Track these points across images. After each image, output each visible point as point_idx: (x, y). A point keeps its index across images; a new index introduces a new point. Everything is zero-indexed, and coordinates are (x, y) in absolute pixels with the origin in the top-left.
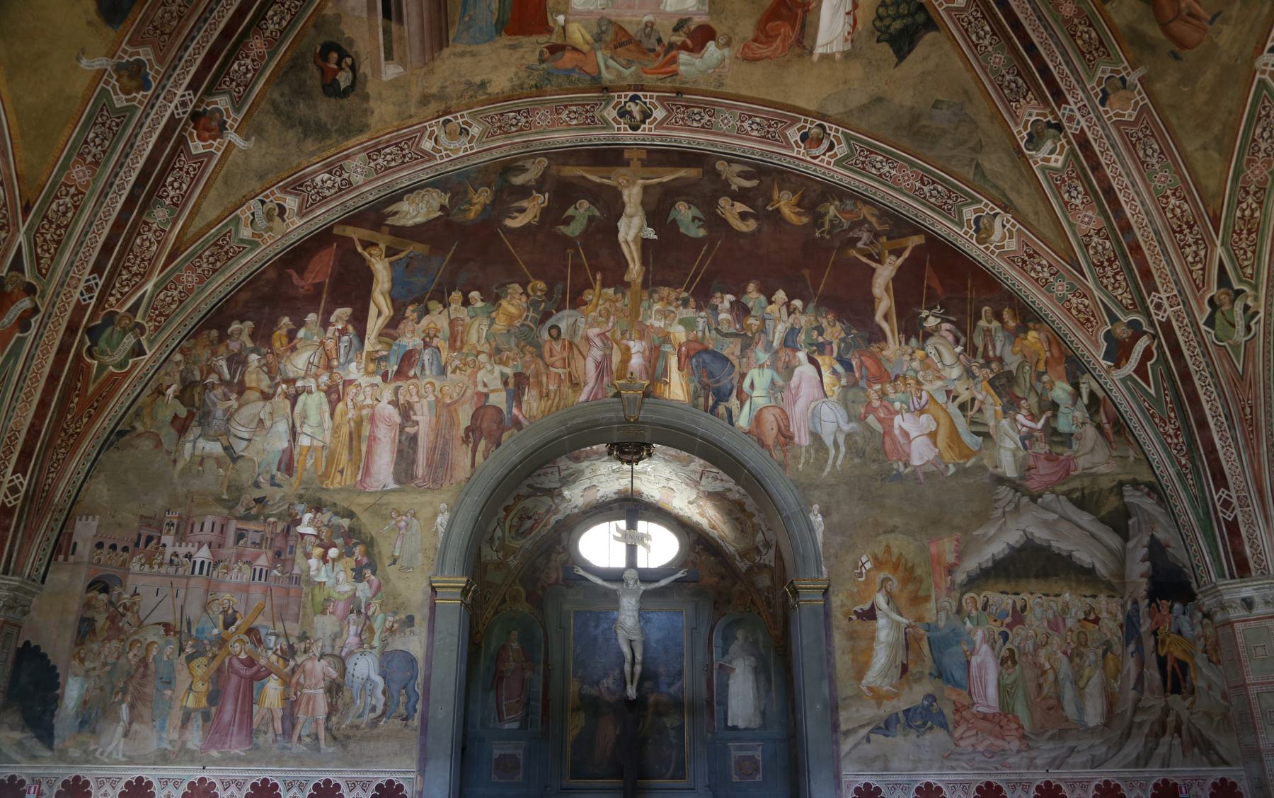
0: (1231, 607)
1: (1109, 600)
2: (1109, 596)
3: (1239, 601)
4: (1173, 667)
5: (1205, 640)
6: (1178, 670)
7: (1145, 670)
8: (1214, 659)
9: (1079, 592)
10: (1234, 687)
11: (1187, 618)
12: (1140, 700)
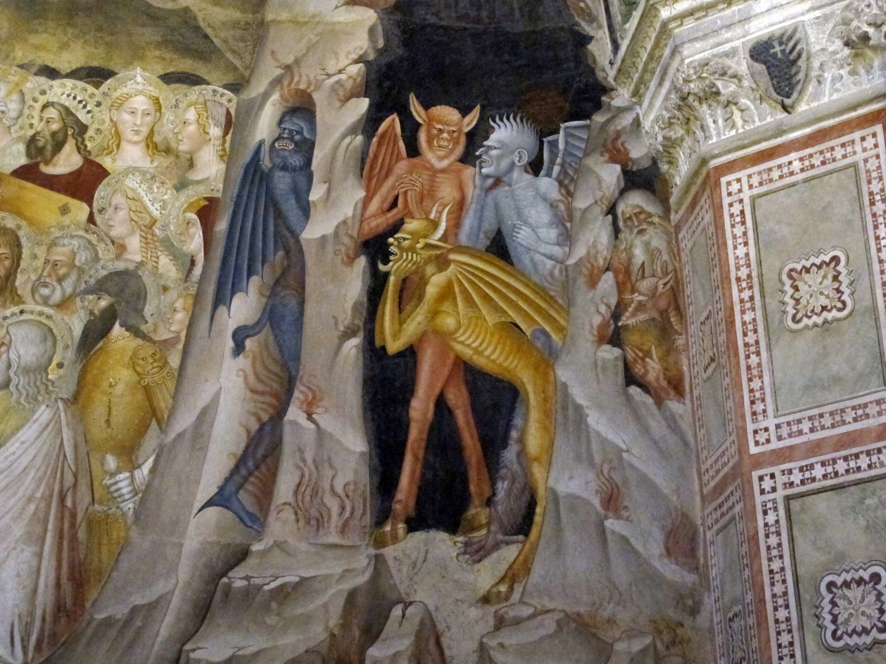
0: (712, 95)
1: (168, 94)
2: (168, 78)
4: (441, 404)
5: (621, 287)
6: (463, 418)
7: (295, 413)
8: (653, 369)
9: (20, 54)
11: (547, 184)
12: (241, 555)
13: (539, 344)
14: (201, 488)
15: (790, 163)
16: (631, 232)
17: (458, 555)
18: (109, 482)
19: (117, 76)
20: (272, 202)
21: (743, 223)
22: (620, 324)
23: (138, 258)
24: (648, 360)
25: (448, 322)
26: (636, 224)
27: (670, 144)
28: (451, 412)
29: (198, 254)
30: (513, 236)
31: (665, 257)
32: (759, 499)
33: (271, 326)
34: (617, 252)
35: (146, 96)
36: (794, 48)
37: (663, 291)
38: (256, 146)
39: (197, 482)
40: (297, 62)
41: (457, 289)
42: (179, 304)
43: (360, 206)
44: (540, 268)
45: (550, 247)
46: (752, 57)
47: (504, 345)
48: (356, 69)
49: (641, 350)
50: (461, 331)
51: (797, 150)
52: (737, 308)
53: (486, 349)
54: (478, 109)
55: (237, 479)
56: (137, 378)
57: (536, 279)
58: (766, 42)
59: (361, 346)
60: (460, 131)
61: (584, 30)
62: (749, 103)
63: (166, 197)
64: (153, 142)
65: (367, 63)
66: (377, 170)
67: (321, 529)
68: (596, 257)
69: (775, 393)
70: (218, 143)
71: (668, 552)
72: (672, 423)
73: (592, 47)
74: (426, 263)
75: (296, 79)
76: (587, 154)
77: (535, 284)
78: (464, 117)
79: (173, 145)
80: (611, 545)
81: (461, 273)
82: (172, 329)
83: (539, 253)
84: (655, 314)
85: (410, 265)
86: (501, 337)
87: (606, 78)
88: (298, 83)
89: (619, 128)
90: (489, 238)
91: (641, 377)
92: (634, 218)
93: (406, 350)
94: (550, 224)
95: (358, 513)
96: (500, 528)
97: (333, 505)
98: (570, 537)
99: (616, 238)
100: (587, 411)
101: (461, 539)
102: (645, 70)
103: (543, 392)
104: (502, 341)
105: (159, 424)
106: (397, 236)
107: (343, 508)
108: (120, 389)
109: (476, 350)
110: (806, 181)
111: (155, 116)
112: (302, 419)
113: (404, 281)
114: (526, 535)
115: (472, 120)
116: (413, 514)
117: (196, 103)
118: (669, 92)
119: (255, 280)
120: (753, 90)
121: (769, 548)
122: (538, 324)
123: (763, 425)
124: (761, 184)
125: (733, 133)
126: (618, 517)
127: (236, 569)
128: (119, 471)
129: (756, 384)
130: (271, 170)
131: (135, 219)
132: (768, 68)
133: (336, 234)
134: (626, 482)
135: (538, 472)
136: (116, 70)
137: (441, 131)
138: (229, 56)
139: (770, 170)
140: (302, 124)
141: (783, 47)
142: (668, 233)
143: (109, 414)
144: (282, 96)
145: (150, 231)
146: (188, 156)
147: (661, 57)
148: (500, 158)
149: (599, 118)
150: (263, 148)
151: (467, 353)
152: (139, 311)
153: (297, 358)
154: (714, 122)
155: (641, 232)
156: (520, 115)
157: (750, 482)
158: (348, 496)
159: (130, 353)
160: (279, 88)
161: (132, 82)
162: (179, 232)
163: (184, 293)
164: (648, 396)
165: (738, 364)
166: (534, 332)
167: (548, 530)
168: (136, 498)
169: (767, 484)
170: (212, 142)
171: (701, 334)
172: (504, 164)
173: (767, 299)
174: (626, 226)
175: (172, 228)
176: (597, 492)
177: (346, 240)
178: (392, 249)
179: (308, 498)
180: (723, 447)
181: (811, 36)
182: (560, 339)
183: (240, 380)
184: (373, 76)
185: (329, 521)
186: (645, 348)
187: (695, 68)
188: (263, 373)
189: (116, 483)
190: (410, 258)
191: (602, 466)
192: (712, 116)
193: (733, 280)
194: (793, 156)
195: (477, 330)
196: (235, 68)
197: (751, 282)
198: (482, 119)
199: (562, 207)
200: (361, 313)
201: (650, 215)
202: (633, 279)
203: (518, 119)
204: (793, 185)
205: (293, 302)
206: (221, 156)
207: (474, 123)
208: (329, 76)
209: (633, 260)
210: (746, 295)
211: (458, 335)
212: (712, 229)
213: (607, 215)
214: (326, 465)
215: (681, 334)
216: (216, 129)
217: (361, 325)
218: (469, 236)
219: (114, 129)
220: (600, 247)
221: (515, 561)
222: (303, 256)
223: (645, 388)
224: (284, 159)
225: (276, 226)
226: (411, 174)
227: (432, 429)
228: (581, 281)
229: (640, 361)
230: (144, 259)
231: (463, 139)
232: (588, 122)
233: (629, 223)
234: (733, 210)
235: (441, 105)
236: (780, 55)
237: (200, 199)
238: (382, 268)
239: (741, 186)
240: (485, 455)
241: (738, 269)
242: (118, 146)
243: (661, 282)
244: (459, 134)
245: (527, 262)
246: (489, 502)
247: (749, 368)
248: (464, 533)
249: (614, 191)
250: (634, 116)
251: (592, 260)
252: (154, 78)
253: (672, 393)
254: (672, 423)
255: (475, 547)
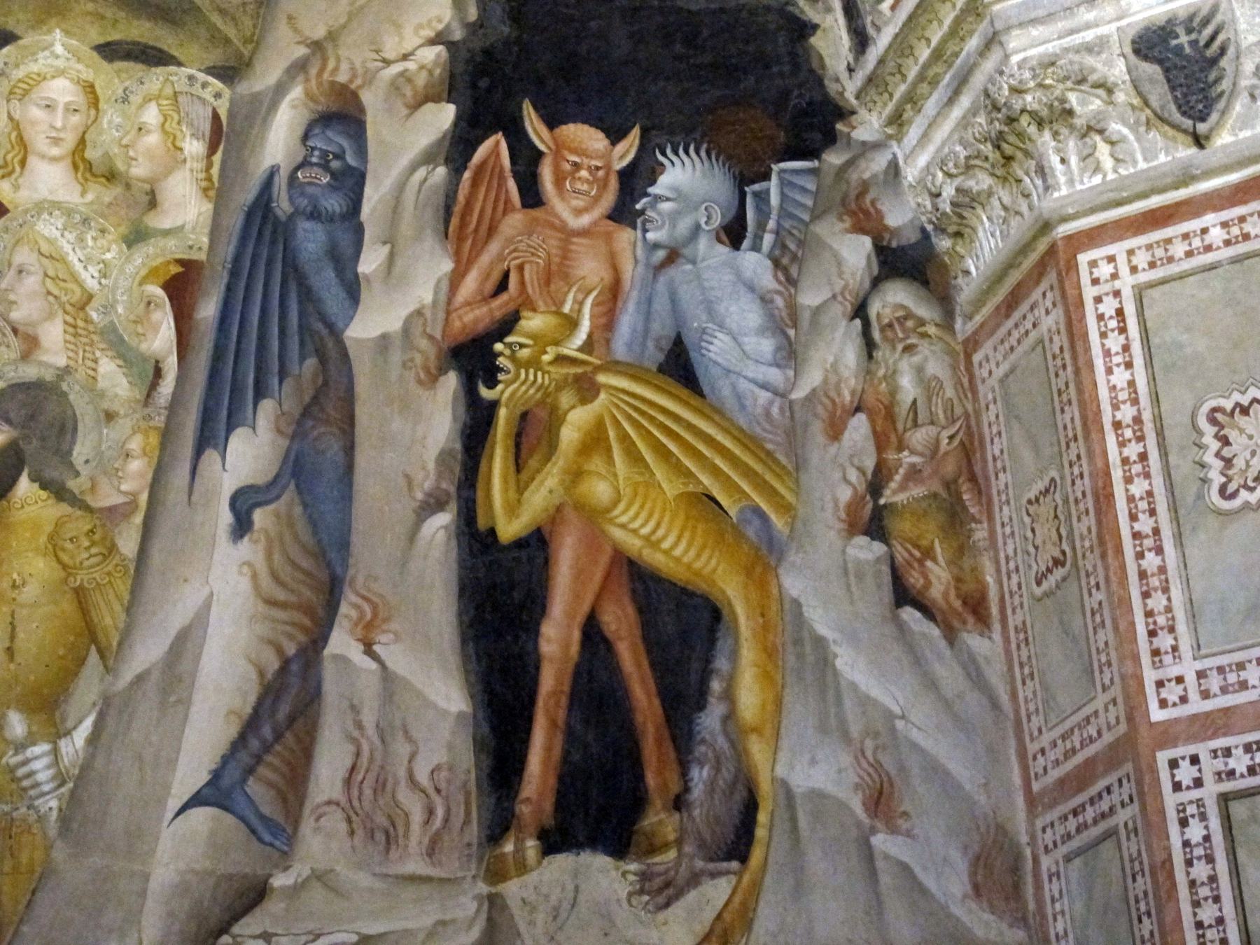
1: (110, 77)
2: (109, 51)
3: (1118, 71)
4: (593, 634)
5: (880, 441)
7: (342, 642)
10: (1067, 786)
13: (751, 532)
14: (179, 774)
15: (1205, 231)
16: (894, 348)
17: (630, 895)
18: (14, 761)
19: (21, 42)
20: (294, 271)
21: (1123, 330)
22: (882, 501)
23: (62, 361)
24: (929, 564)
25: (599, 490)
26: (901, 335)
27: (967, 201)
28: (608, 645)
29: (166, 357)
30: (701, 348)
31: (950, 392)
32: (1171, 800)
33: (297, 486)
34: (872, 379)
35: (72, 80)
36: (1213, 38)
37: (949, 448)
38: (265, 176)
39: (172, 763)
40: (332, 36)
41: (612, 434)
42: (135, 444)
43: (445, 286)
44: (748, 403)
45: (763, 368)
46: (1137, 52)
47: (695, 527)
48: (432, 54)
49: (917, 547)
50: (621, 506)
51: (1216, 209)
52: (1117, 474)
53: (664, 537)
54: (636, 133)
55: (244, 757)
56: (63, 574)
57: (742, 422)
58: (1162, 28)
59: (453, 528)
60: (608, 167)
61: (802, 12)
62: (1125, 131)
63: (108, 256)
64: (84, 159)
65: (451, 46)
66: (472, 226)
67: (393, 847)
68: (838, 384)
69: (1193, 616)
70: (200, 165)
71: (977, 889)
72: (974, 672)
73: (817, 41)
74: (559, 388)
75: (331, 64)
76: (817, 215)
77: (741, 430)
78: (614, 143)
79: (120, 166)
80: (885, 880)
81: (618, 407)
82: (124, 487)
83: (745, 377)
84: (937, 487)
85: (532, 391)
86: (687, 518)
87: (842, 94)
88: (336, 69)
89: (866, 175)
90: (661, 349)
91: (919, 592)
92: (897, 326)
93: (531, 535)
94: (761, 331)
95: (458, 820)
96: (699, 846)
97: (414, 807)
98: (816, 862)
99: (870, 357)
100: (835, 649)
101: (633, 867)
102: (921, 77)
103: (763, 615)
104: (690, 524)
105: (102, 655)
106: (509, 339)
107: (431, 812)
108: (30, 592)
109: (647, 539)
110: (1236, 260)
111: (88, 116)
112: (355, 653)
113: (524, 416)
114: (744, 859)
115: (628, 151)
116: (549, 821)
117: (158, 97)
118: (973, 112)
119: (267, 407)
120: (1133, 108)
121: (1192, 884)
122: (748, 497)
123: (1174, 671)
124: (1152, 265)
125: (1097, 179)
126: (893, 830)
127: (243, 921)
128: (31, 740)
129: (1157, 602)
130: (291, 217)
131: (56, 291)
132: (1167, 71)
133: (406, 330)
134: (902, 769)
135: (757, 750)
136: (18, 31)
137: (576, 166)
138: (216, 19)
139: (1168, 241)
140: (345, 143)
141: (1193, 36)
142: (951, 353)
143: (13, 637)
144: (309, 95)
145: (81, 314)
146: (147, 187)
147: (956, 55)
148: (674, 217)
149: (833, 158)
150: (276, 179)
151: (632, 544)
152: (65, 457)
153: (344, 545)
154: (1063, 161)
155: (909, 349)
156: (705, 146)
157: (1154, 770)
158: (438, 791)
159: (49, 528)
160: (301, 78)
161: (47, 53)
162: (132, 317)
163: (143, 424)
164: (932, 625)
165: (1123, 567)
166: (741, 511)
167: (779, 852)
168: (63, 790)
169: (1186, 773)
170: (188, 165)
171: (1027, 520)
172: (684, 226)
173: (1171, 458)
174: (885, 338)
175: (120, 310)
176: (857, 787)
177: (424, 343)
178: (502, 361)
179: (368, 792)
180: (1088, 710)
181: (1242, 20)
182: (786, 523)
183: (245, 584)
184: (460, 68)
185: (406, 835)
186: (924, 543)
187: (1033, 69)
188: (286, 573)
189: (26, 762)
190: (531, 377)
191: (862, 742)
192: (1058, 151)
193: (1108, 427)
194: (1210, 219)
195: (648, 506)
196: (227, 41)
197: (1141, 430)
198: (644, 148)
199: (779, 302)
200: (452, 471)
201: (922, 322)
202: (900, 426)
203: (703, 154)
204: (1212, 267)
205: (333, 447)
206: (205, 190)
207: (630, 157)
208: (387, 63)
209: (898, 397)
210: (1133, 451)
211: (616, 512)
212: (1061, 340)
213: (853, 318)
214: (400, 736)
215: (980, 522)
216: (195, 143)
217: (452, 490)
218: (629, 345)
219: (14, 135)
220: (846, 373)
221: (726, 905)
222: (350, 369)
223: (927, 610)
224: (314, 202)
225: (302, 315)
226: (530, 235)
227: (577, 673)
228: (817, 430)
229: (916, 565)
230: (72, 363)
231: (614, 184)
232: (816, 163)
233: (889, 334)
234: (1102, 308)
235: (574, 122)
236: (1188, 50)
237: (169, 262)
238: (485, 393)
239: (1116, 268)
240: (668, 719)
241: (1116, 407)
242: (23, 163)
243: (945, 434)
244: (607, 174)
245: (726, 392)
246: (679, 803)
247: (1143, 575)
248: (639, 858)
249: (862, 279)
250: (890, 157)
251: (833, 394)
252: (86, 51)
253: (971, 620)
254: (974, 672)
255: (658, 882)
